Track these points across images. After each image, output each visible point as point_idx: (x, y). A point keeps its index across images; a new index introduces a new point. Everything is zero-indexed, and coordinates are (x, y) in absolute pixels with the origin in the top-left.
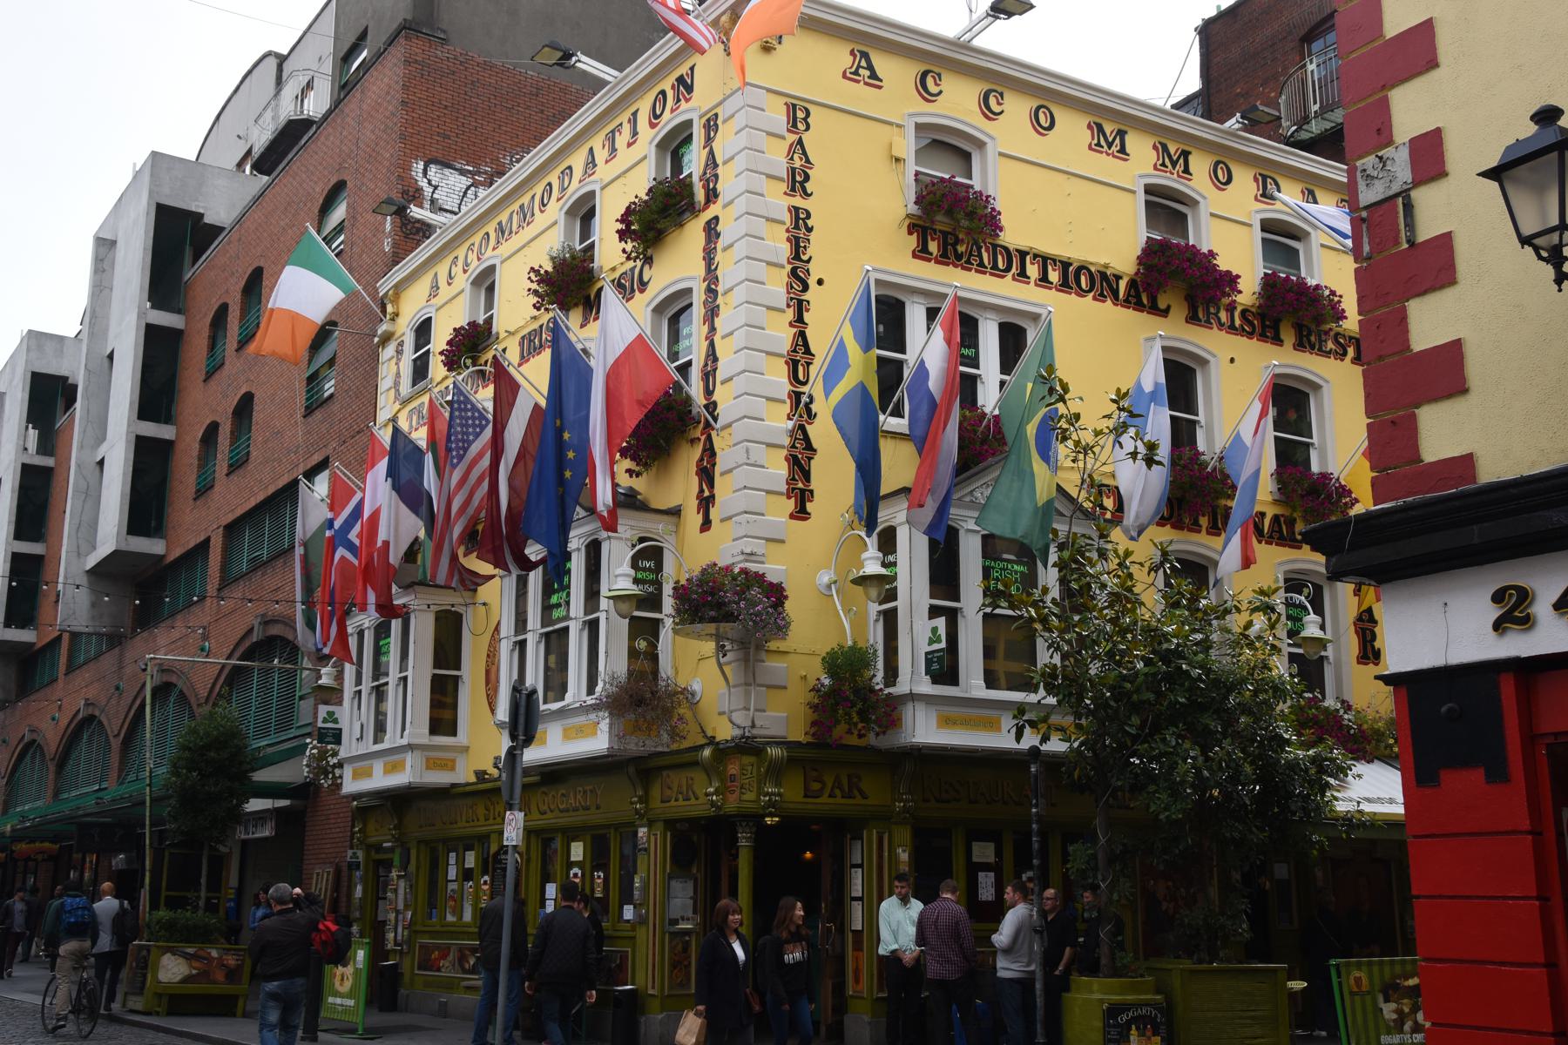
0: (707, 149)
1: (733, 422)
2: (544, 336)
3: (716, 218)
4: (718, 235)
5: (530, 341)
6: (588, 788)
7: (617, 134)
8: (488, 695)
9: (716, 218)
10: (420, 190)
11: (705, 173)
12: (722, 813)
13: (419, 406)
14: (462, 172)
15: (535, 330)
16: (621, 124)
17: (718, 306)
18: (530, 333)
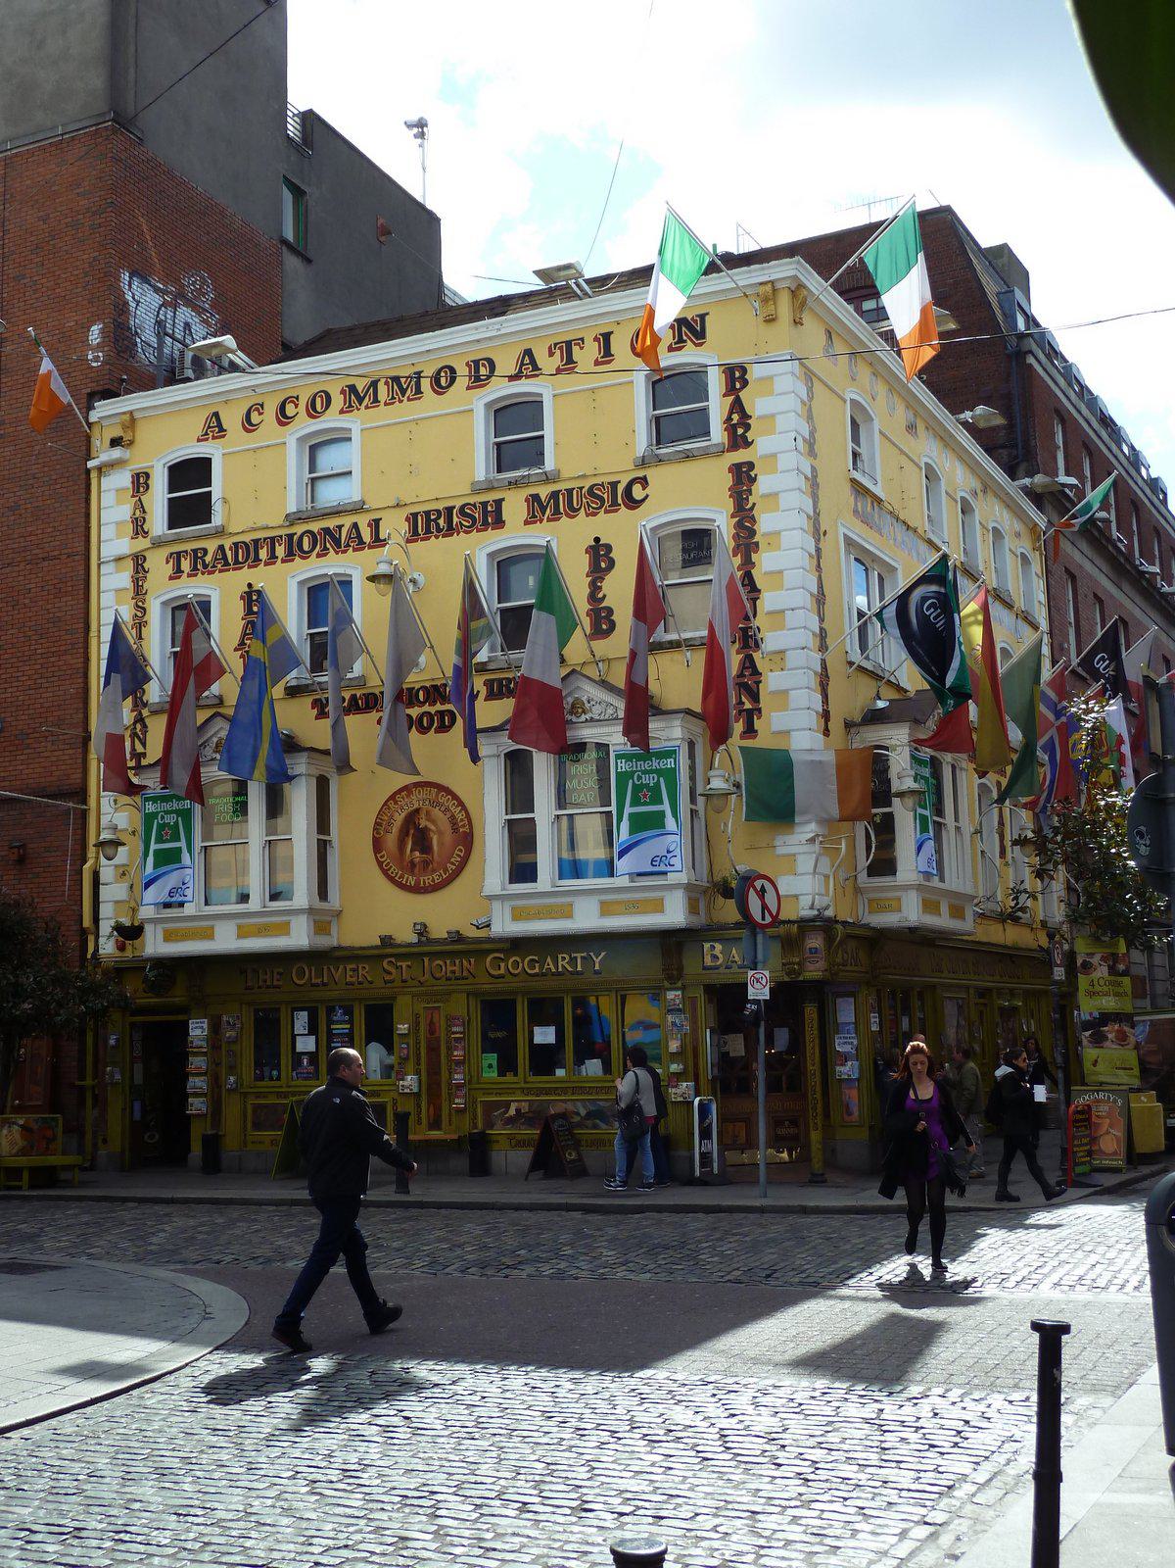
0: (731, 399)
1: (787, 650)
2: (455, 520)
3: (751, 465)
4: (753, 480)
5: (428, 521)
6: (578, 955)
7: (575, 349)
8: (380, 864)
9: (751, 465)
10: (126, 303)
11: (729, 419)
12: (801, 978)
13: (195, 551)
14: (157, 290)
15: (438, 511)
16: (582, 339)
17: (757, 544)
18: (427, 513)
